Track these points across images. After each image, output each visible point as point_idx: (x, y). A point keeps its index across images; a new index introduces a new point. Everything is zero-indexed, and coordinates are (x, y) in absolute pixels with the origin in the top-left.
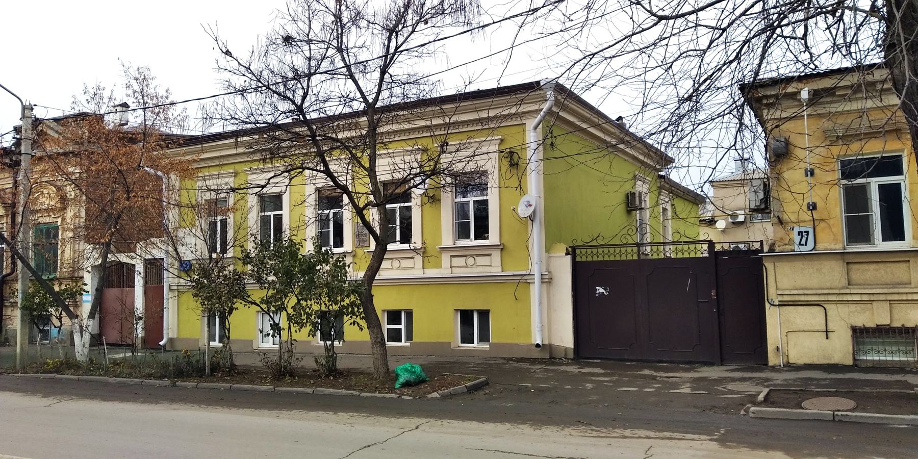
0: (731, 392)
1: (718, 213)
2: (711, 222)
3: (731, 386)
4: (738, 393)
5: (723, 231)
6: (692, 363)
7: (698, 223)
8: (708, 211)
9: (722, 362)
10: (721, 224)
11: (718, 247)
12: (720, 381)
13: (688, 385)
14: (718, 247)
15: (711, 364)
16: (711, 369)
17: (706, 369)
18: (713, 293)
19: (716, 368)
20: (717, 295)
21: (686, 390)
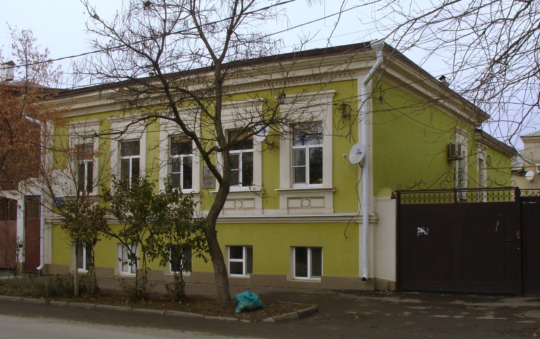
0: (527, 318)
1: (527, 164)
2: (522, 173)
3: (528, 314)
4: (534, 319)
5: (532, 181)
6: (498, 295)
7: (510, 173)
8: (519, 163)
9: (523, 295)
10: (530, 174)
11: (523, 194)
12: (520, 309)
13: (492, 313)
14: (523, 194)
15: (513, 295)
16: (513, 299)
17: (509, 299)
18: (518, 234)
19: (517, 299)
20: (521, 235)
21: (490, 317)
